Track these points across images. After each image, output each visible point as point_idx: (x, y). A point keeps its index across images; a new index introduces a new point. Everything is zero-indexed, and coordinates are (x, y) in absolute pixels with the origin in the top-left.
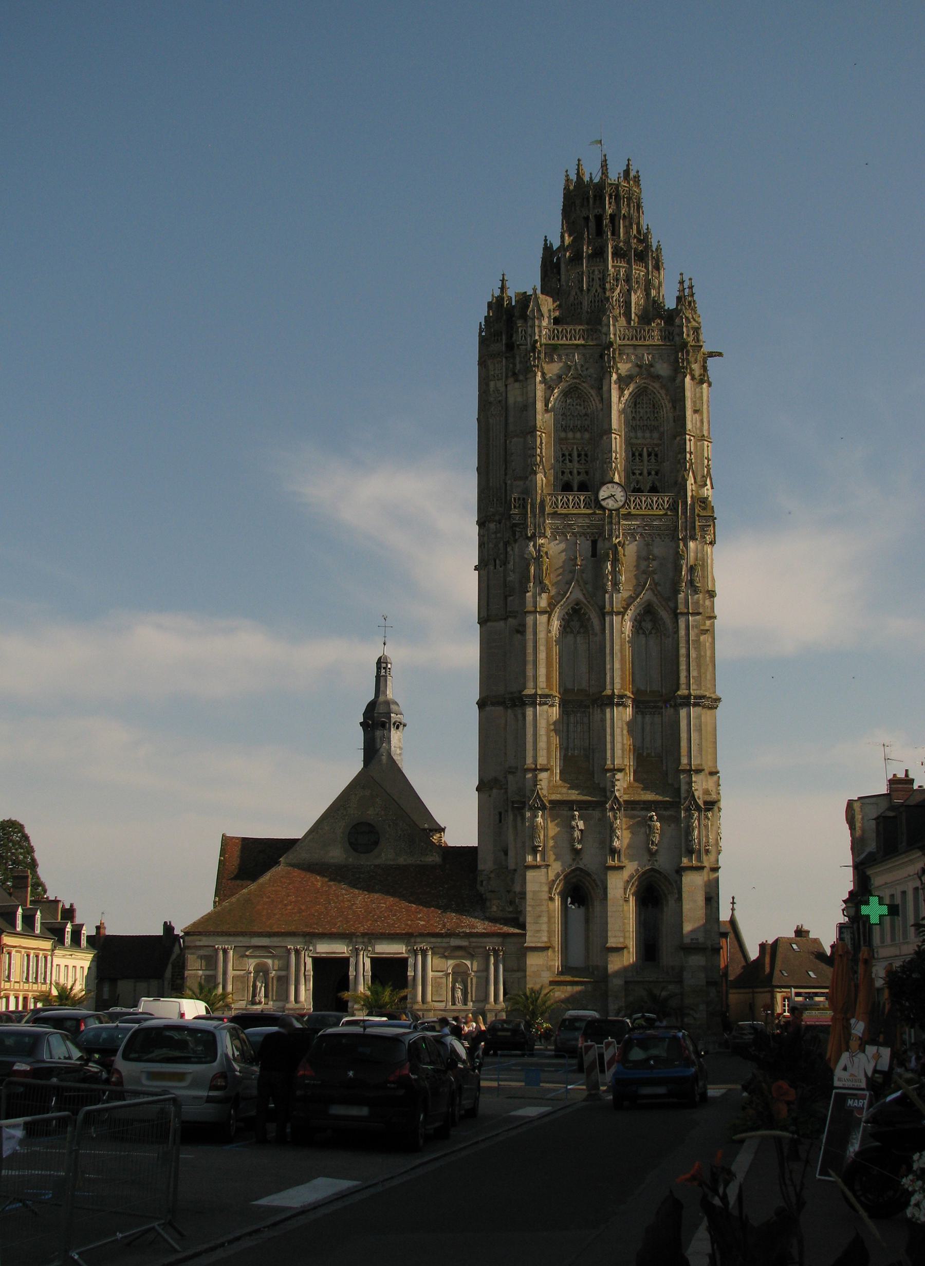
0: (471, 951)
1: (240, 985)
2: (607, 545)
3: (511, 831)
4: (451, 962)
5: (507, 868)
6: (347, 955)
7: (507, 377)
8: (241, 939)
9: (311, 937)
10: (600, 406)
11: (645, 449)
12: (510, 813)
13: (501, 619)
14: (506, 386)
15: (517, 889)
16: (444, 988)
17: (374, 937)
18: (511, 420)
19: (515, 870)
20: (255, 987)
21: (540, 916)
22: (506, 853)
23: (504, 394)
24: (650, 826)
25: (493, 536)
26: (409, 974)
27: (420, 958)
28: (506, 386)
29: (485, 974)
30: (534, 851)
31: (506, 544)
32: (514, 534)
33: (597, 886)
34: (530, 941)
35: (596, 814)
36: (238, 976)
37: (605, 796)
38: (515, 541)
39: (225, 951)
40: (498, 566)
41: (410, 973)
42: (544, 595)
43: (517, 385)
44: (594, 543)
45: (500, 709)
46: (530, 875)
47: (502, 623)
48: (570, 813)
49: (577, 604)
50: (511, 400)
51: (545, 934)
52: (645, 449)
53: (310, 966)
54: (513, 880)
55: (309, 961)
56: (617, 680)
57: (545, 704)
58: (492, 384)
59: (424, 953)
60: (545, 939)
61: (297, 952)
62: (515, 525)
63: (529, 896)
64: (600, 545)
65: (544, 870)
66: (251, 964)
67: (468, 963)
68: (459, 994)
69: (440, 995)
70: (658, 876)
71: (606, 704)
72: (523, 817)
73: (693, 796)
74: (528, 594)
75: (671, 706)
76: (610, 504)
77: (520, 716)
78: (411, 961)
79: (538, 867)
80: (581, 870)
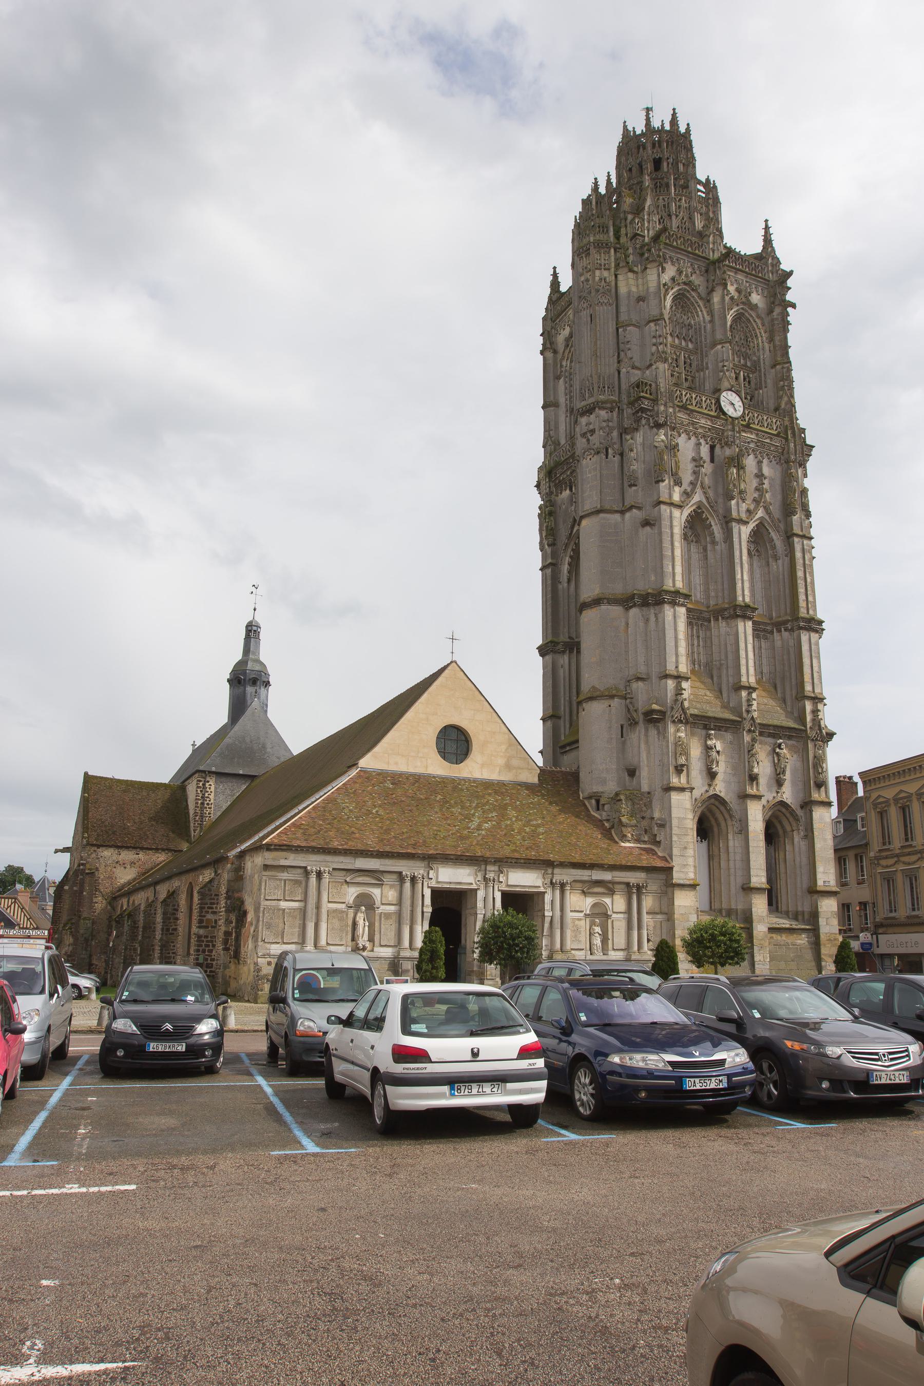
0: (610, 885)
1: (336, 923)
2: (728, 452)
3: (643, 746)
4: (590, 901)
5: (639, 790)
6: (474, 886)
7: (617, 266)
8: (341, 859)
9: (432, 859)
10: (708, 318)
11: (742, 373)
12: (641, 727)
13: (617, 512)
14: (616, 276)
15: (657, 815)
17: (506, 862)
18: (623, 309)
19: (649, 793)
20: (355, 924)
21: (685, 848)
22: (632, 772)
23: (613, 284)
24: (778, 754)
25: (604, 424)
27: (558, 892)
28: (616, 276)
30: (679, 770)
31: (624, 431)
32: (638, 421)
33: (731, 816)
34: (678, 876)
35: (729, 736)
36: (335, 911)
37: (741, 716)
38: (637, 430)
39: (319, 875)
40: (610, 456)
41: (548, 914)
42: (677, 489)
43: (630, 275)
44: (712, 448)
45: (617, 610)
46: (675, 797)
47: (617, 517)
48: (704, 732)
49: (699, 507)
50: (623, 290)
51: (692, 869)
52: (742, 373)
53: (428, 901)
54: (649, 805)
55: (428, 893)
56: (747, 592)
57: (683, 605)
58: (597, 273)
59: (562, 886)
60: (692, 875)
61: (413, 879)
62: (643, 410)
63: (675, 822)
64: (718, 450)
65: (687, 794)
66: (351, 893)
67: (608, 901)
68: (597, 941)
69: (580, 941)
70: (784, 810)
71: (738, 616)
72: (663, 734)
73: (820, 726)
74: (662, 485)
75: (785, 630)
76: (730, 411)
77: (652, 618)
78: (548, 898)
79: (682, 789)
80: (716, 797)
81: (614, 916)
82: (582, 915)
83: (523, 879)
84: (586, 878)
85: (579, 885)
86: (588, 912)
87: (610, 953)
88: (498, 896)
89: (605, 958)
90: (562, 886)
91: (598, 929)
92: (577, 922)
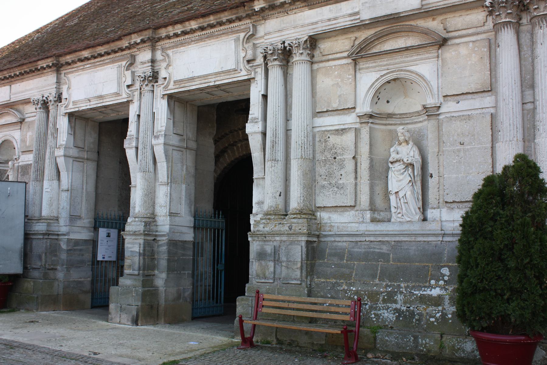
16: (350, 166)
26: (250, 128)
27: (276, 73)
29: (488, 101)
67: (425, 67)
68: (399, 181)
69: (340, 187)
81: (449, 107)
82: (350, 119)
83: (204, 60)
84: (346, 22)
85: (343, 44)
86: (364, 107)
87: (431, 214)
88: (162, 107)
89: (417, 228)
90: (286, 54)
91: (408, 152)
92: (334, 140)
